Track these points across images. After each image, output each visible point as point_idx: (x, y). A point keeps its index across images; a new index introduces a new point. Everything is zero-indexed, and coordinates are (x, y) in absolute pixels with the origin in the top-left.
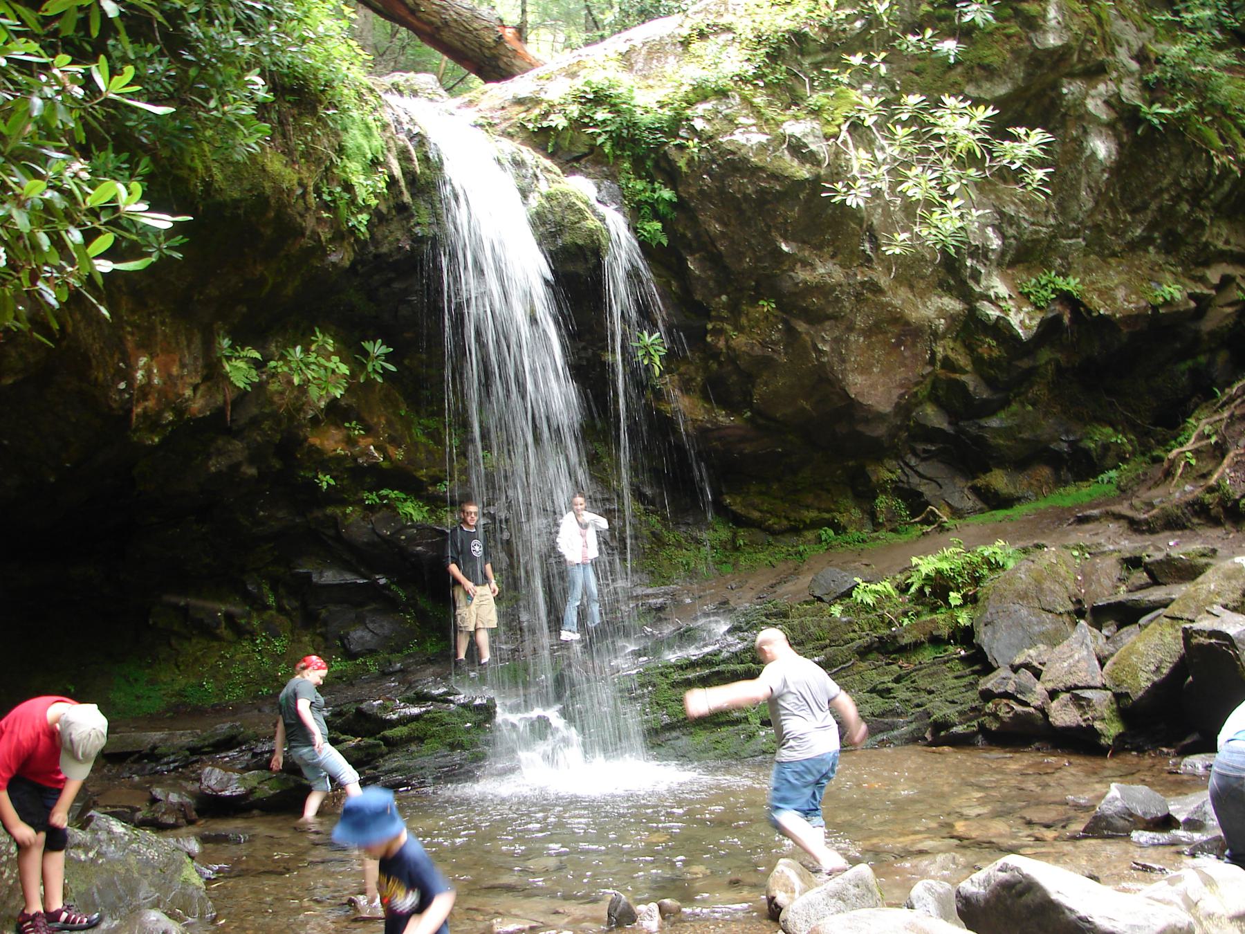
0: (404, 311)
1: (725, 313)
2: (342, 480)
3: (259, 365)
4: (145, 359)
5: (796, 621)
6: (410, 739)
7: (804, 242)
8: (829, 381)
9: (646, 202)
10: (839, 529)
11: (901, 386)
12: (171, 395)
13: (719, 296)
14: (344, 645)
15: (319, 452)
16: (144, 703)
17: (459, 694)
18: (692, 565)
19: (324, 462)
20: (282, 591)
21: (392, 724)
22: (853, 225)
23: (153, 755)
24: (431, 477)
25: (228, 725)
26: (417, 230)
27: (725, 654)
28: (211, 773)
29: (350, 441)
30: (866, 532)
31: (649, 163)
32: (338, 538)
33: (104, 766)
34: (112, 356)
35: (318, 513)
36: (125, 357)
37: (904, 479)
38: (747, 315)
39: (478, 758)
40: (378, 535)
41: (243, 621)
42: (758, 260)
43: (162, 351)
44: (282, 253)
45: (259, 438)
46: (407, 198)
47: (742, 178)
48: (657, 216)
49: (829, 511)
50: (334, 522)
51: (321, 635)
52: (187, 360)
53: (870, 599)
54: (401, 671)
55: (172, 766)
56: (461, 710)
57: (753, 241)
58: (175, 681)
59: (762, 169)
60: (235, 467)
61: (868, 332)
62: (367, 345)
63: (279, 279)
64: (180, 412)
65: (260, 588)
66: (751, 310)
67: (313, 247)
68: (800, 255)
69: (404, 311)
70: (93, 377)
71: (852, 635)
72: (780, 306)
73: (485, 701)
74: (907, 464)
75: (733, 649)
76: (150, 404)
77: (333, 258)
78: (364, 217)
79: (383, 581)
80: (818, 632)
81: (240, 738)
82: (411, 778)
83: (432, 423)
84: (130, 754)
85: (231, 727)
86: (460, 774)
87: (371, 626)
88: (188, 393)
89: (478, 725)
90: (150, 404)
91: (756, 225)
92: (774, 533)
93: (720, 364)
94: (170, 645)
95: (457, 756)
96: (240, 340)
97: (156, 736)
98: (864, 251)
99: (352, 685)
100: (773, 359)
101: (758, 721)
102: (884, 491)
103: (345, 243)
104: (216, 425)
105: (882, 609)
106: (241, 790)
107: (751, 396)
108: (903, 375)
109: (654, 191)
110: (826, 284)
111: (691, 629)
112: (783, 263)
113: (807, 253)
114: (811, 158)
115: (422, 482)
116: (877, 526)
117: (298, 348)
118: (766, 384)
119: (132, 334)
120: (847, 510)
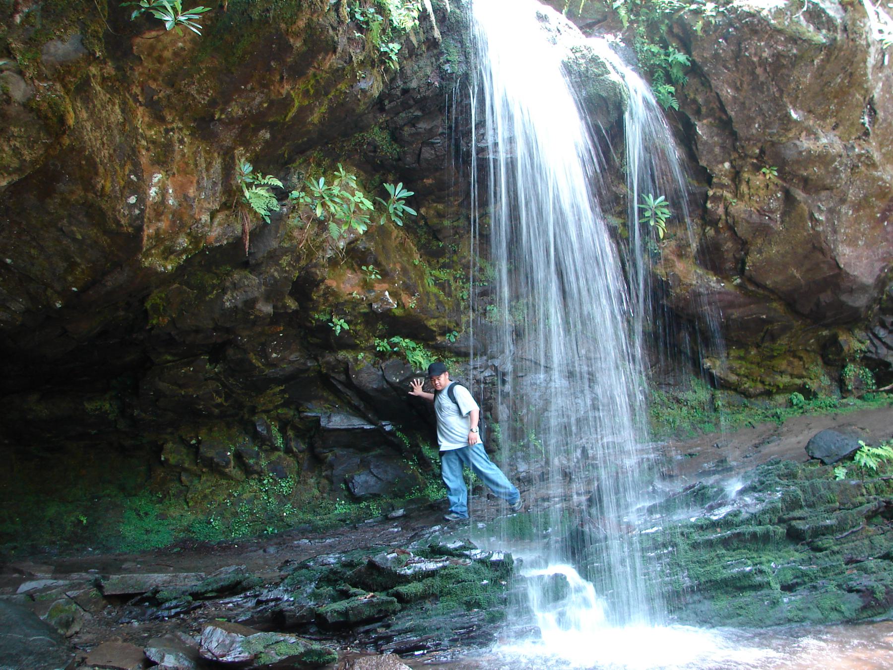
0: (427, 153)
1: (726, 181)
2: (356, 325)
3: (281, 195)
4: (160, 176)
5: (807, 483)
6: (424, 596)
7: (810, 112)
8: (822, 251)
9: (659, 66)
10: (809, 394)
11: (883, 259)
12: (186, 218)
13: (722, 162)
14: (348, 489)
15: (335, 294)
16: (154, 537)
17: (476, 548)
18: (677, 423)
19: (338, 309)
20: (290, 433)
21: (405, 580)
22: (858, 96)
23: (153, 599)
24: (440, 327)
25: (233, 568)
26: (447, 67)
27: (744, 515)
28: (212, 633)
29: (367, 286)
30: (835, 399)
31: (663, 28)
32: (349, 384)
33: (104, 607)
34: (122, 167)
35: (330, 358)
36: (137, 168)
37: (873, 349)
38: (748, 182)
39: (495, 619)
40: (387, 381)
41: (251, 461)
42: (766, 125)
43: (178, 171)
44: (311, 71)
45: (276, 274)
46: (437, 33)
47: (759, 41)
48: (669, 80)
49: (800, 377)
50: (346, 369)
51: (327, 477)
52: (205, 183)
53: (873, 463)
54: (403, 516)
55: (173, 611)
56: (478, 566)
57: (764, 106)
58: (181, 517)
59: (780, 32)
60: (250, 303)
61: (858, 207)
62: (389, 187)
63: (307, 103)
64: (195, 239)
65: (269, 429)
66: (751, 177)
67: (343, 69)
68: (806, 124)
69: (427, 153)
70: (99, 186)
71: (860, 498)
72: (782, 175)
73: (502, 557)
74: (876, 336)
75: (752, 510)
76: (163, 225)
77: (363, 85)
78: (396, 46)
79: (388, 428)
80: (830, 495)
81: (244, 583)
82: (426, 640)
83: (443, 275)
84: (132, 596)
85: (237, 571)
86: (479, 636)
87: (375, 471)
88: (205, 218)
89: (495, 582)
90: (163, 225)
91: (768, 90)
92: (746, 394)
93: (717, 231)
94: (181, 482)
95: (476, 616)
96: (261, 165)
97: (157, 578)
98: (863, 124)
99: (355, 528)
100: (771, 228)
101: (778, 586)
102: (853, 360)
103: (376, 70)
104: (234, 255)
105: (884, 473)
106: (245, 656)
107: (744, 263)
108: (885, 249)
109: (667, 55)
110: (828, 153)
111: (704, 488)
112: (790, 130)
113: (811, 123)
114: (830, 23)
115: (435, 332)
116: (844, 391)
117: (322, 180)
118: (760, 252)
119: (148, 150)
120: (817, 377)
